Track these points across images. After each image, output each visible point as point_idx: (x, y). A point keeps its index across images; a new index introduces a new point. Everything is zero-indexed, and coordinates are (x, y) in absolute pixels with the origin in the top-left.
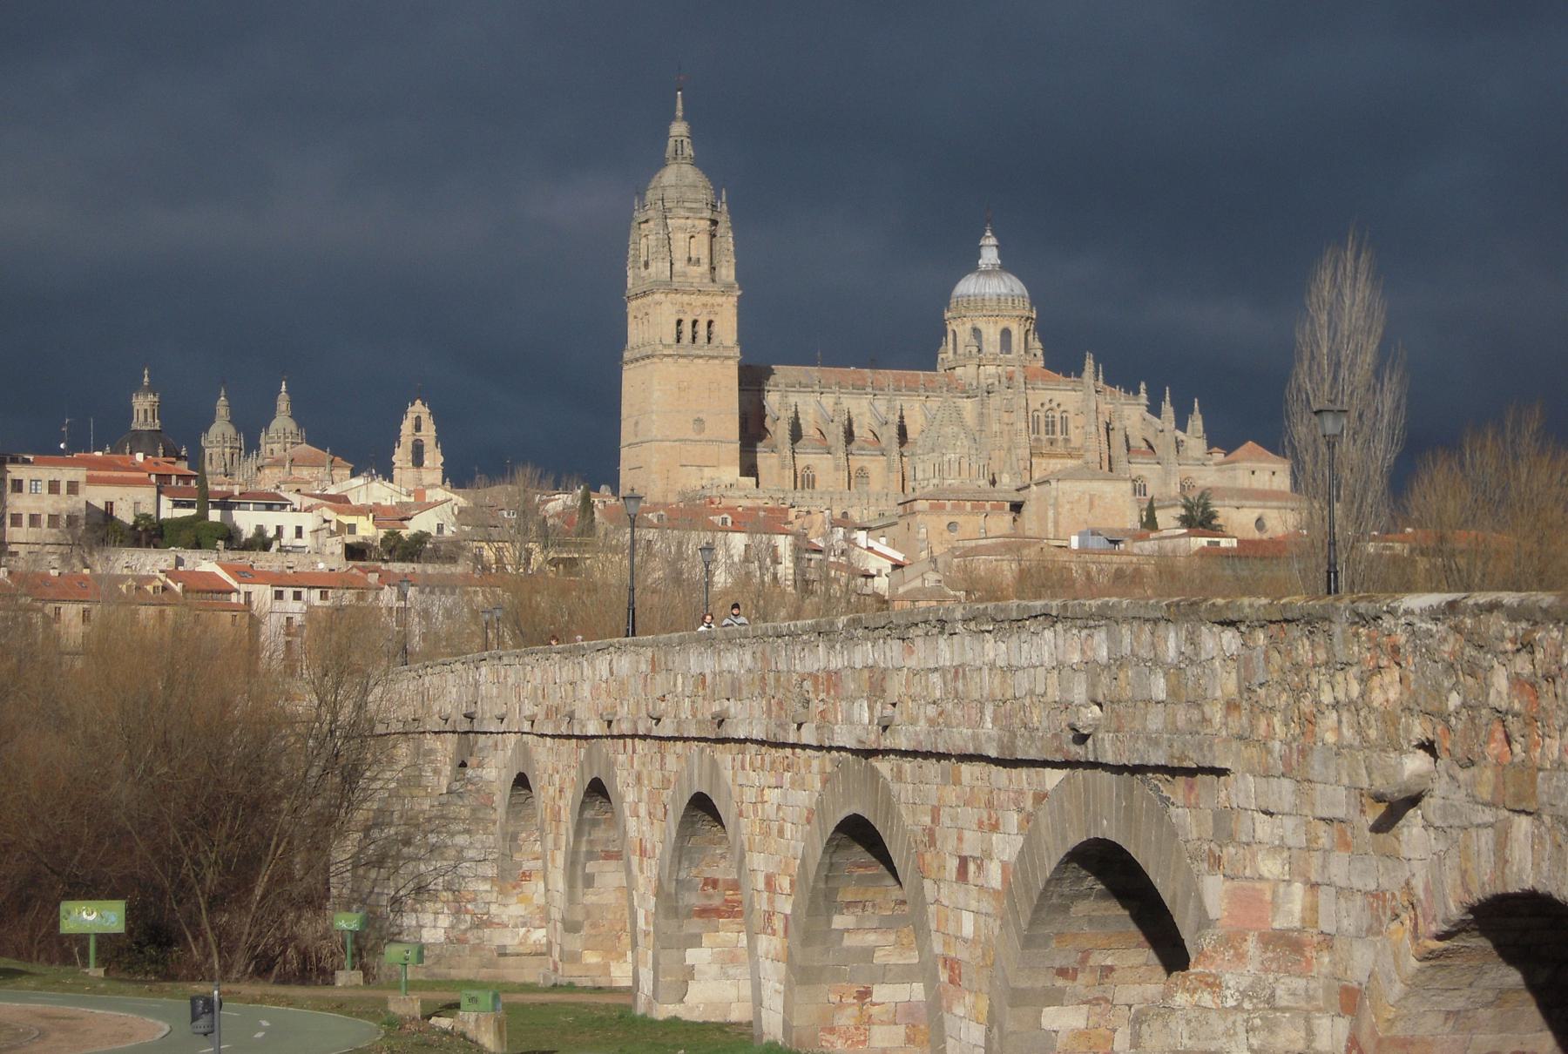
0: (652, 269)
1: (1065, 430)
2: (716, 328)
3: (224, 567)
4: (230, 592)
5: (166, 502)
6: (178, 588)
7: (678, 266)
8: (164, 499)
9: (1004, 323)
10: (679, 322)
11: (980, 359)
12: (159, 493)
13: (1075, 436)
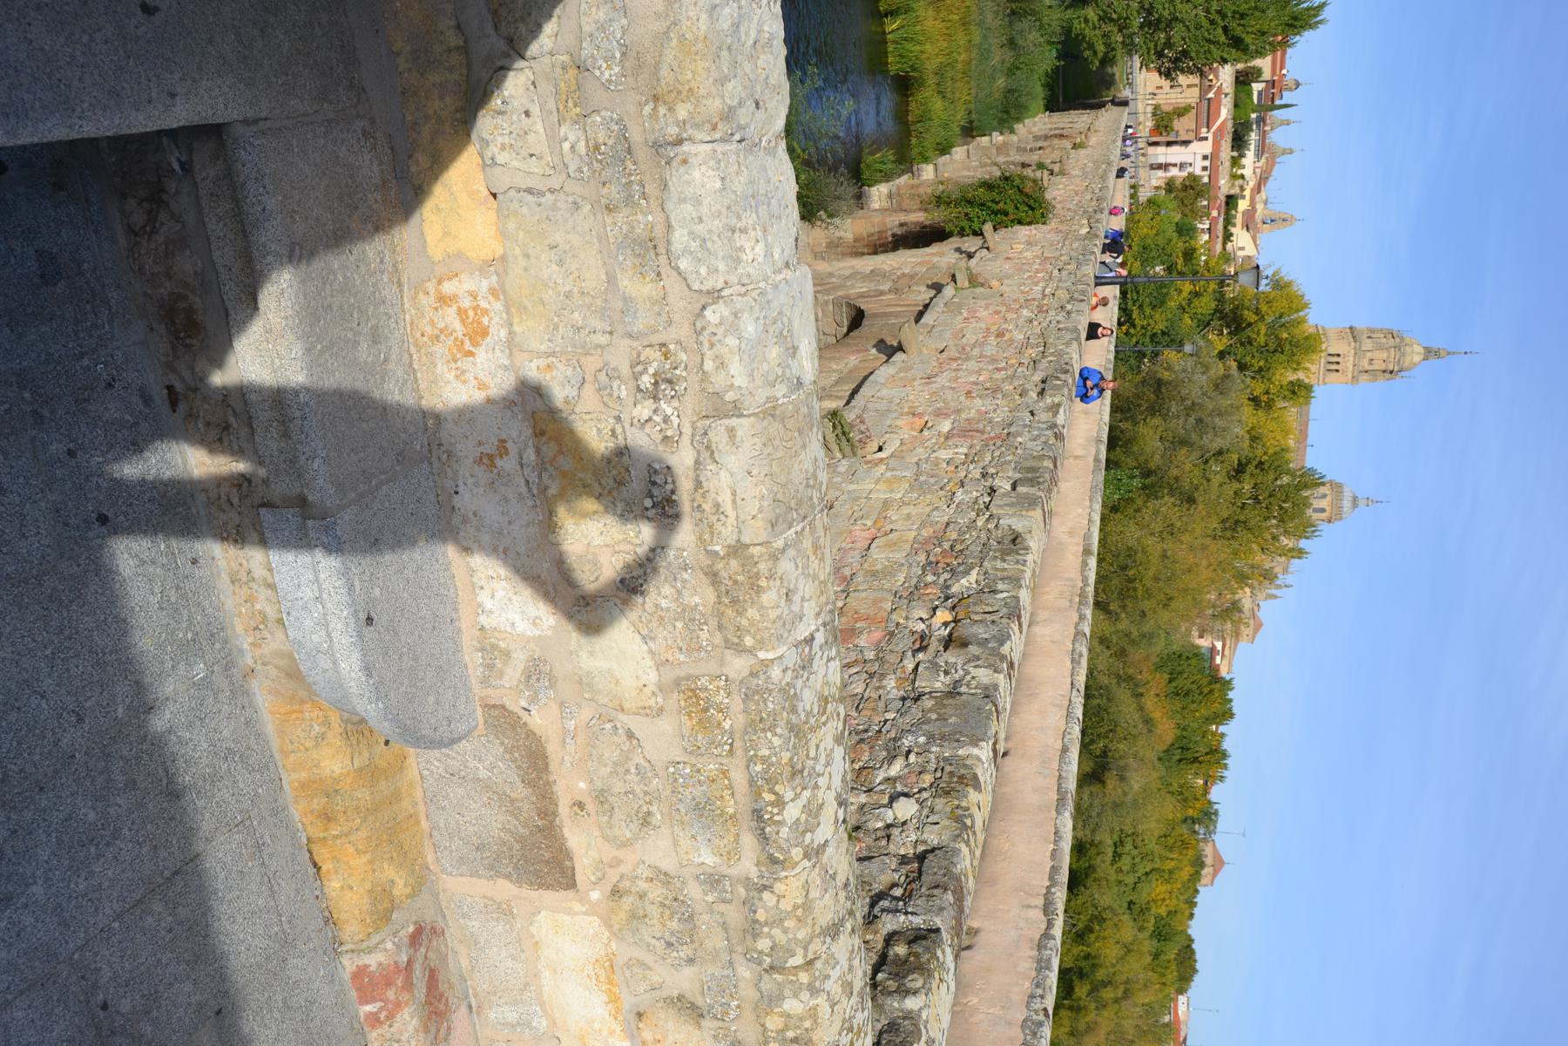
0: (1369, 341)
2: (1335, 374)
3: (1226, 120)
7: (1369, 354)
8: (1263, 85)
9: (1328, 509)
10: (1339, 355)
12: (1267, 82)
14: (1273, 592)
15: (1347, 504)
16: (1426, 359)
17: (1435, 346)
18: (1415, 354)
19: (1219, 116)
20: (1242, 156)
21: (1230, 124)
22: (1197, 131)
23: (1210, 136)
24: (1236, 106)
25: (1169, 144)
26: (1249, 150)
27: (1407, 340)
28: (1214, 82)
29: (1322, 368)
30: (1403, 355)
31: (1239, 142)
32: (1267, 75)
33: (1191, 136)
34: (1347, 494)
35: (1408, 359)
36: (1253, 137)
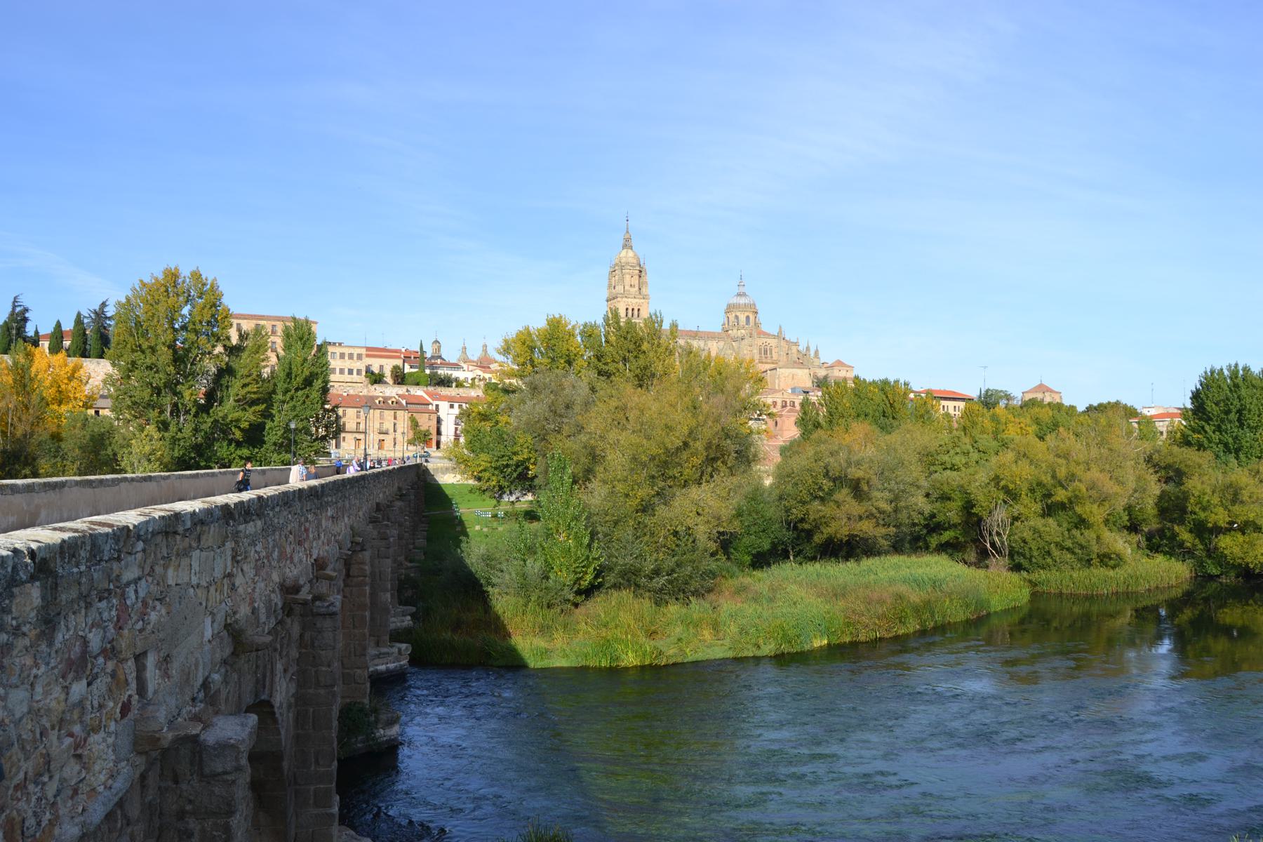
0: (617, 288)
1: (771, 353)
2: (641, 311)
3: (427, 393)
4: (428, 405)
5: (407, 366)
6: (404, 402)
7: (627, 288)
8: (406, 364)
9: (746, 314)
10: (627, 309)
12: (404, 362)
13: (775, 356)
14: (812, 353)
15: (742, 301)
16: (631, 248)
17: (622, 242)
18: (627, 255)
19: (421, 397)
20: (456, 380)
21: (431, 389)
22: (431, 412)
23: (435, 403)
24: (418, 384)
25: (439, 433)
26: (451, 375)
27: (617, 261)
28: (394, 400)
30: (627, 263)
31: (445, 382)
32: (399, 362)
33: (434, 418)
34: (735, 300)
35: (631, 260)
36: (442, 372)
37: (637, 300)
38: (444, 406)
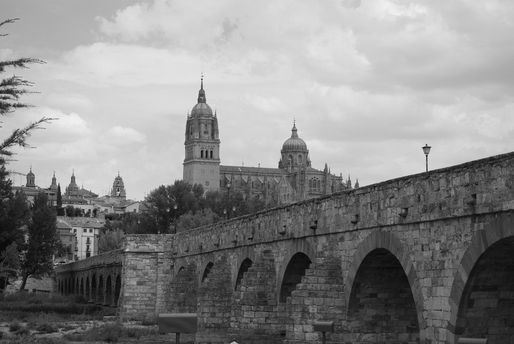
1: (319, 187)
2: (214, 154)
7: (202, 134)
10: (202, 152)
11: (292, 165)
15: (296, 142)
29: (210, 161)
37: (210, 144)
38: (80, 230)
